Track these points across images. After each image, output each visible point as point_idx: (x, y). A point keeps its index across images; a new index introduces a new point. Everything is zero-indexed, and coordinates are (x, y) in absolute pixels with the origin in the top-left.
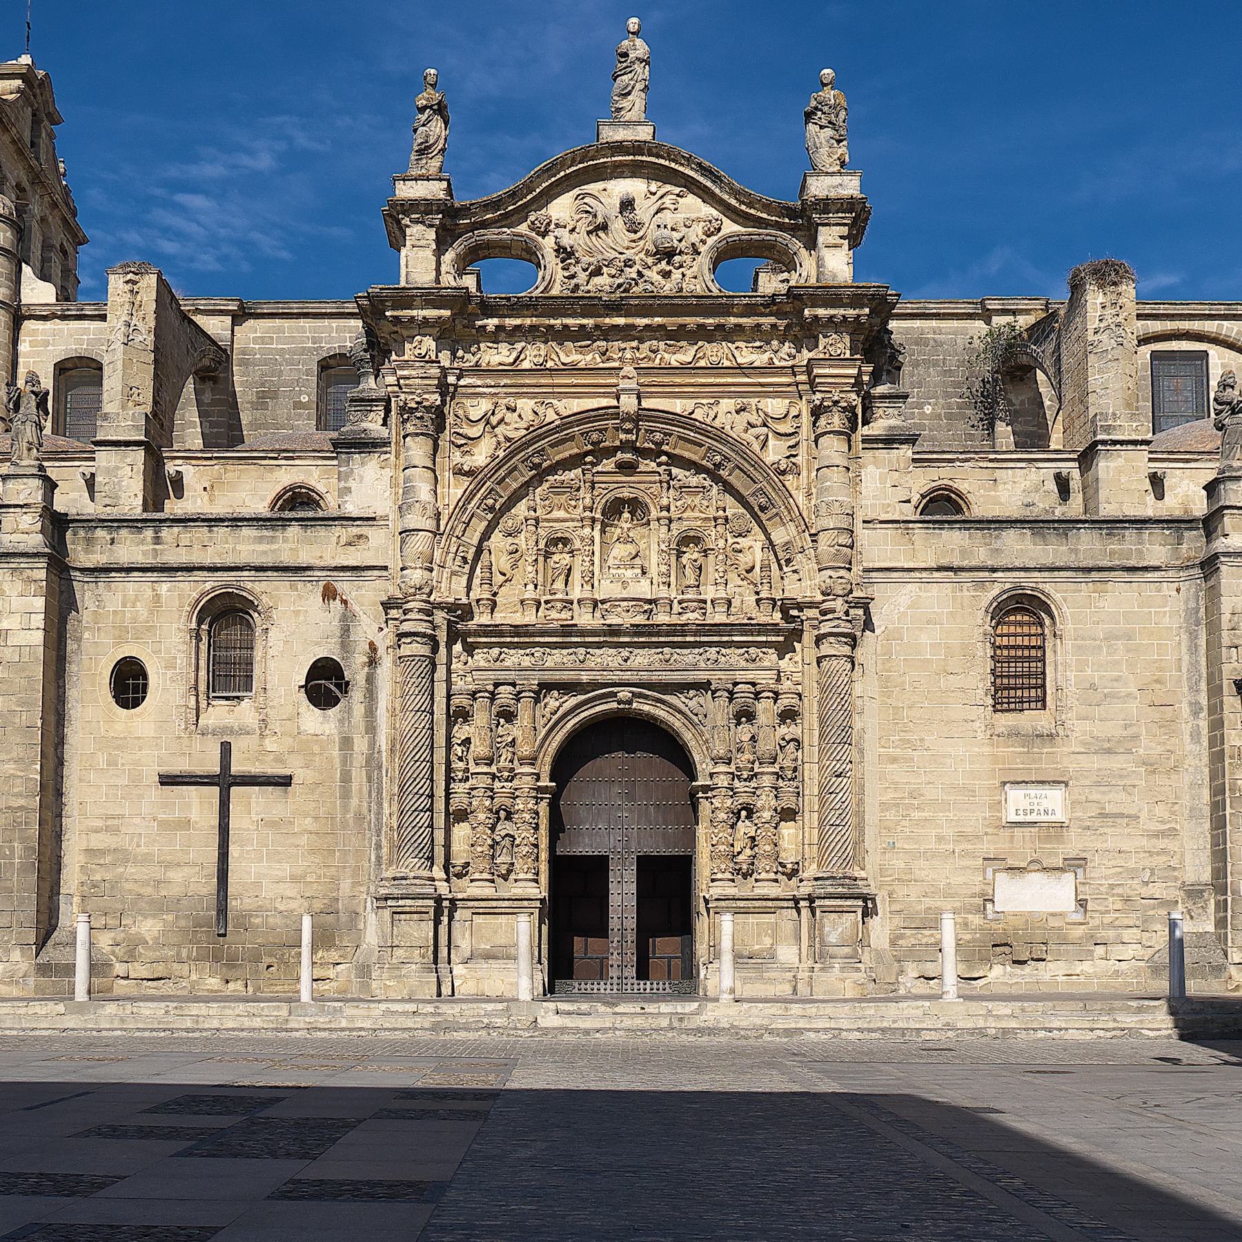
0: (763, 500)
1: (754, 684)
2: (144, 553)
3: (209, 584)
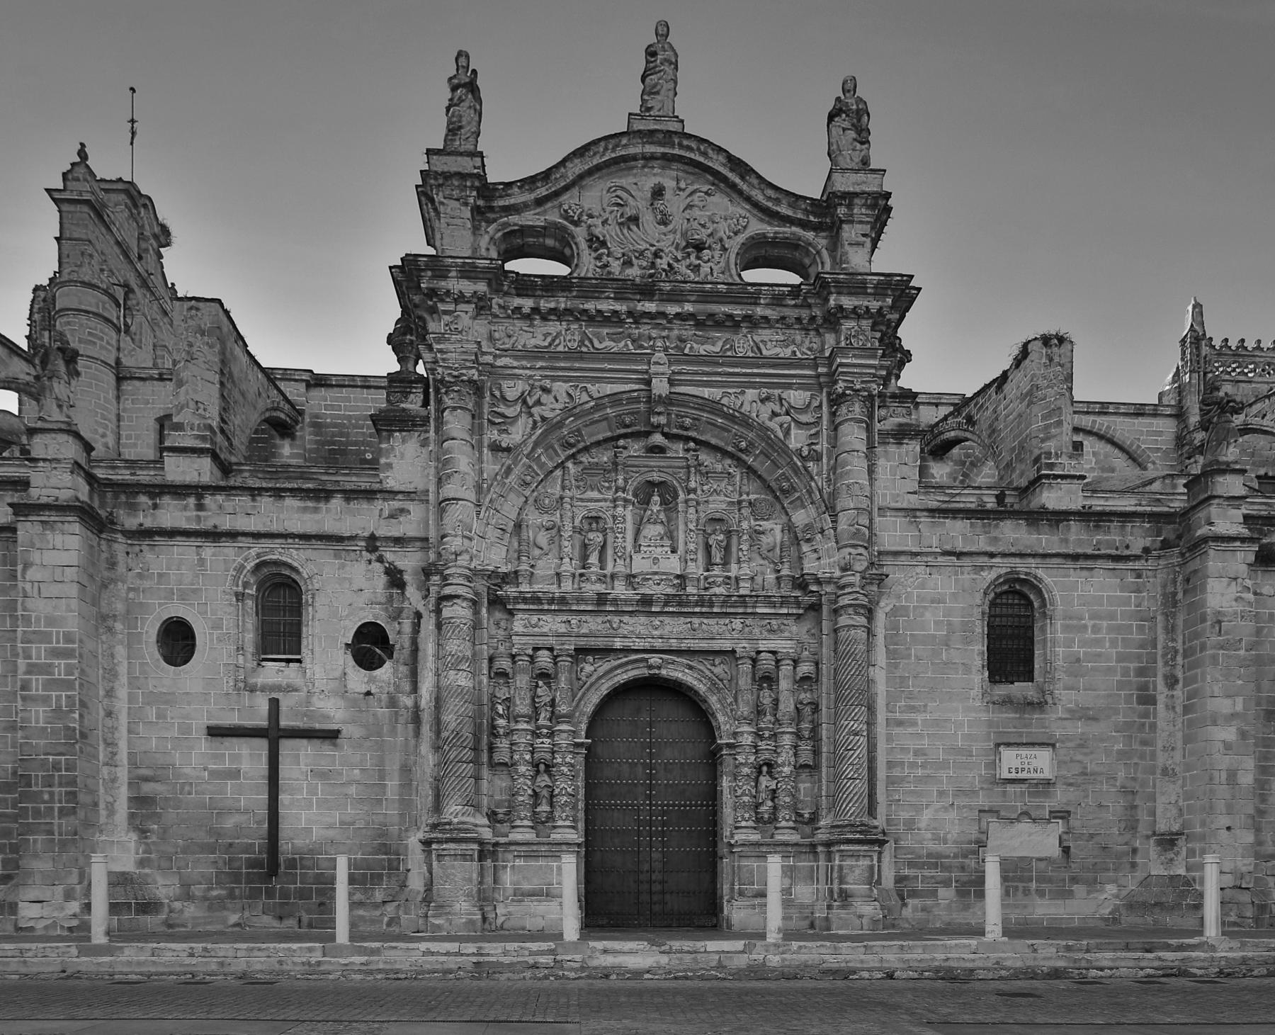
0: (785, 485)
1: (774, 653)
2: (188, 519)
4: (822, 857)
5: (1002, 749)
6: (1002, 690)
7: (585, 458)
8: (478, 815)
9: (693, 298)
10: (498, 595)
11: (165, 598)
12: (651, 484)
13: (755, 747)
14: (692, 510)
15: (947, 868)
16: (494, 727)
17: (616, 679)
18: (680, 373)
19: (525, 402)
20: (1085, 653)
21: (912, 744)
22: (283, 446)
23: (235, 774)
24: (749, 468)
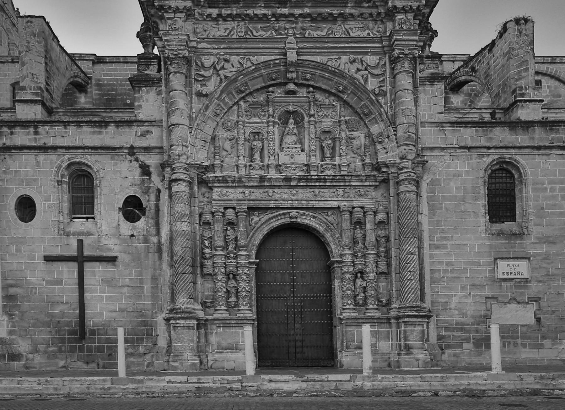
2: (30, 140)
3: (66, 157)
4: (394, 325)
5: (498, 261)
6: (497, 227)
7: (250, 99)
8: (196, 303)
9: (309, 5)
10: (203, 178)
11: (19, 184)
12: (288, 112)
13: (353, 262)
14: (312, 127)
15: (468, 331)
16: (203, 253)
17: (272, 225)
18: (303, 48)
19: (215, 68)
20: (546, 204)
21: (445, 259)
22: (81, 97)
23: (60, 282)
24: (345, 101)
